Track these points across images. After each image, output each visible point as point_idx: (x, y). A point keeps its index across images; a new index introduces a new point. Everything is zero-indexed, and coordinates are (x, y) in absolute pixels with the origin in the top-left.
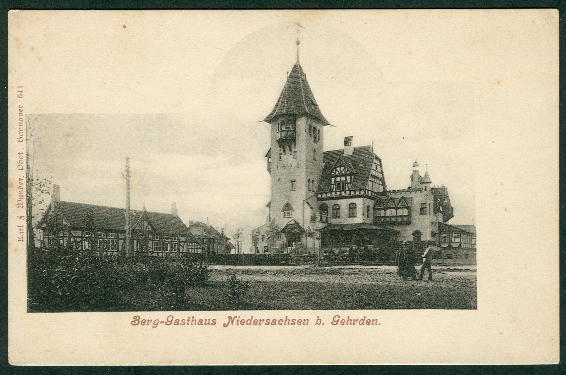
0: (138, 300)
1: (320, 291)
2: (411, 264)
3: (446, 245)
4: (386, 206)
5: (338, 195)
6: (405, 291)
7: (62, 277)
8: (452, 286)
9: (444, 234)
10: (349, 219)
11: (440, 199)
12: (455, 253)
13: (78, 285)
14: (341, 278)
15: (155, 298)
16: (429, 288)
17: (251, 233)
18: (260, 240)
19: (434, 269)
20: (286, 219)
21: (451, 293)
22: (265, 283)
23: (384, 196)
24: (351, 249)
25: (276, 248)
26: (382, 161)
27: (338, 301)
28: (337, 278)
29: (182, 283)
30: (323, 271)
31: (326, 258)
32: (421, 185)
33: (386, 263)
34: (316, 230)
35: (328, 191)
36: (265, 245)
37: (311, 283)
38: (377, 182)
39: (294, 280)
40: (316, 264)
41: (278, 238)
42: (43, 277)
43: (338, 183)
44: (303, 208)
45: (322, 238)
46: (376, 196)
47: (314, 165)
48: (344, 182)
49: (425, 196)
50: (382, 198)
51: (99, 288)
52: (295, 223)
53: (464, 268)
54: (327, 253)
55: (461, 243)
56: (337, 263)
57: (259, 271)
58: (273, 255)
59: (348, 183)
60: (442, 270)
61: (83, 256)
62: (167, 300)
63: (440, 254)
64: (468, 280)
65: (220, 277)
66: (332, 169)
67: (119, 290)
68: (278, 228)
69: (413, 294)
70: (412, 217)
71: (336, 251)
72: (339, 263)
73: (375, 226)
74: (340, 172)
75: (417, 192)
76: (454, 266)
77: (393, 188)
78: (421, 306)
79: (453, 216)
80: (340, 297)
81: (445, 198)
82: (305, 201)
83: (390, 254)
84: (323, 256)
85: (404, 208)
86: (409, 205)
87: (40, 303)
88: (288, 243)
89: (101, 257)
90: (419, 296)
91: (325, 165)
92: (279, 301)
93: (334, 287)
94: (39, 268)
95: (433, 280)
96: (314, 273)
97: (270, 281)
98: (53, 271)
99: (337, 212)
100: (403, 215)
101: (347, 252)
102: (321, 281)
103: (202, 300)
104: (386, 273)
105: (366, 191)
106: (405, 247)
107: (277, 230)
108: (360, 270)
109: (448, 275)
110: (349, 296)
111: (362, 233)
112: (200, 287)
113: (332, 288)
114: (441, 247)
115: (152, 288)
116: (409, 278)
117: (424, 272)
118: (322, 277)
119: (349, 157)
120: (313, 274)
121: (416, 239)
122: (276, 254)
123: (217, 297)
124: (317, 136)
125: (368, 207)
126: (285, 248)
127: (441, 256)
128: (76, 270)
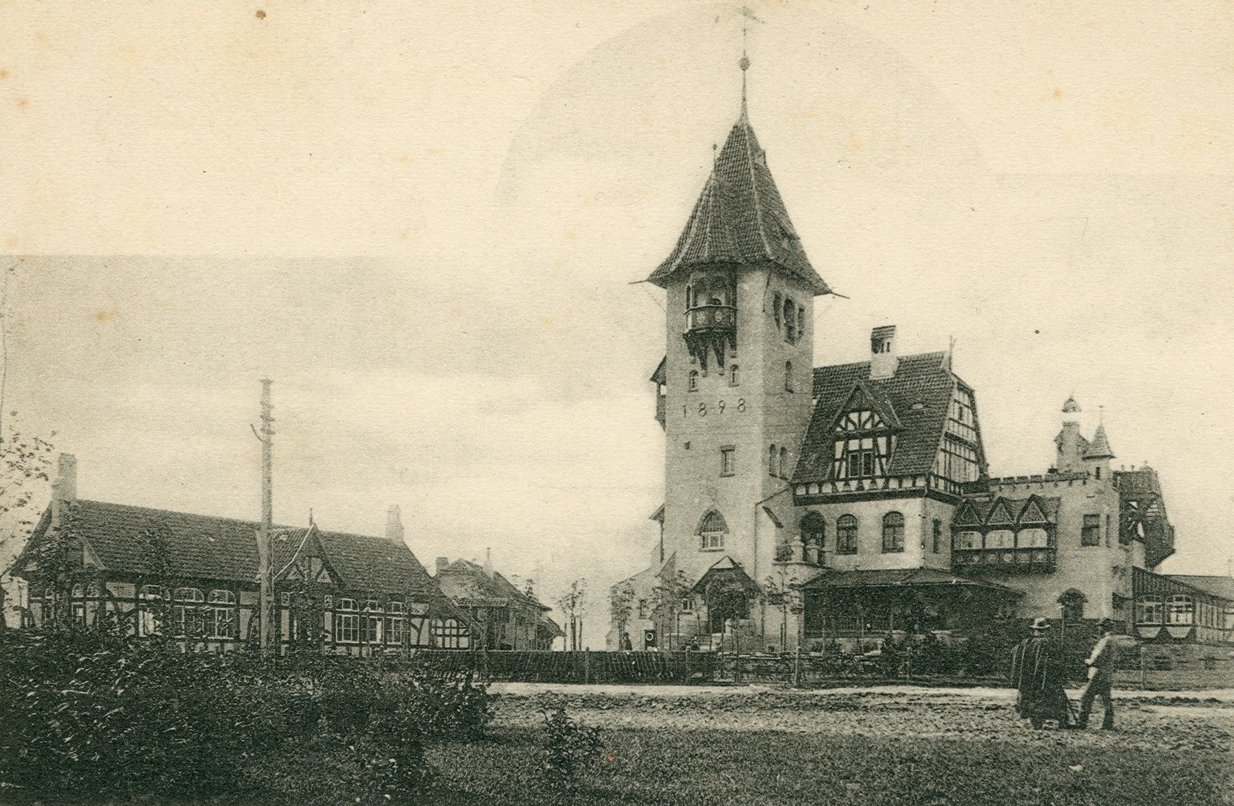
0: (293, 778)
1: (801, 756)
2: (1055, 682)
3: (1153, 633)
4: (987, 520)
5: (853, 489)
6: (1037, 760)
7: (80, 711)
8: (1168, 747)
9: (1149, 599)
10: (882, 556)
11: (1139, 503)
12: (1179, 655)
13: (126, 734)
14: (859, 721)
15: (339, 773)
16: (1104, 752)
17: (608, 593)
18: (634, 614)
19: (1119, 699)
20: (707, 554)
21: (1166, 766)
22: (646, 732)
23: (981, 492)
24: (888, 641)
25: (678, 636)
26: (977, 395)
27: (849, 786)
28: (847, 721)
29: (414, 730)
30: (808, 702)
31: (816, 666)
32: (1085, 464)
33: (984, 679)
34: (792, 587)
35: (826, 477)
36: (648, 626)
37: (776, 733)
38: (962, 455)
39: (727, 726)
40: (790, 682)
41: (685, 607)
42: (27, 709)
43: (853, 456)
44: (756, 525)
45: (806, 609)
46: (959, 494)
47: (787, 405)
48: (871, 453)
49: (1096, 495)
50: (977, 499)
51: (183, 743)
52: (732, 566)
53: (1202, 695)
54: (820, 651)
55: (1194, 625)
56: (848, 678)
57: (630, 700)
58: (671, 655)
59: (880, 457)
60: (1142, 701)
61: (140, 653)
62: (372, 778)
63: (1138, 655)
64: (1213, 730)
65: (522, 714)
66: (836, 416)
67: (238, 750)
68: (685, 580)
69: (1061, 768)
70: (1060, 553)
71: (847, 645)
72: (853, 678)
73: (956, 576)
74: (860, 424)
75: (1074, 482)
76: (1174, 690)
77: (1006, 472)
78: (1082, 800)
79: (1173, 551)
80: (855, 775)
81: (1152, 500)
82: (760, 506)
83: (997, 656)
84: (810, 660)
85: (1037, 526)
86: (1051, 519)
87: (19, 783)
88: (711, 623)
89: (190, 658)
90: (1075, 772)
91: (817, 406)
92: (685, 782)
93: (841, 747)
94: (16, 687)
95: (1116, 730)
96: (784, 707)
97: (661, 728)
98: (55, 694)
99: (849, 538)
100: (1035, 546)
101: (877, 649)
102: (802, 729)
103: (472, 780)
104: (984, 707)
105: (932, 478)
106: (1037, 637)
107: (680, 585)
108: (912, 700)
109: (1159, 716)
110: (881, 771)
111: (920, 595)
112: (465, 743)
113: (834, 748)
114: (1138, 638)
115: (333, 745)
116: (1050, 723)
117: (1090, 707)
118: (806, 718)
119: (885, 385)
120: (782, 710)
121: (1070, 613)
122: (677, 653)
123: (512, 771)
124: (797, 323)
125: (937, 523)
126: (705, 636)
127: (1140, 662)
128: (120, 691)
